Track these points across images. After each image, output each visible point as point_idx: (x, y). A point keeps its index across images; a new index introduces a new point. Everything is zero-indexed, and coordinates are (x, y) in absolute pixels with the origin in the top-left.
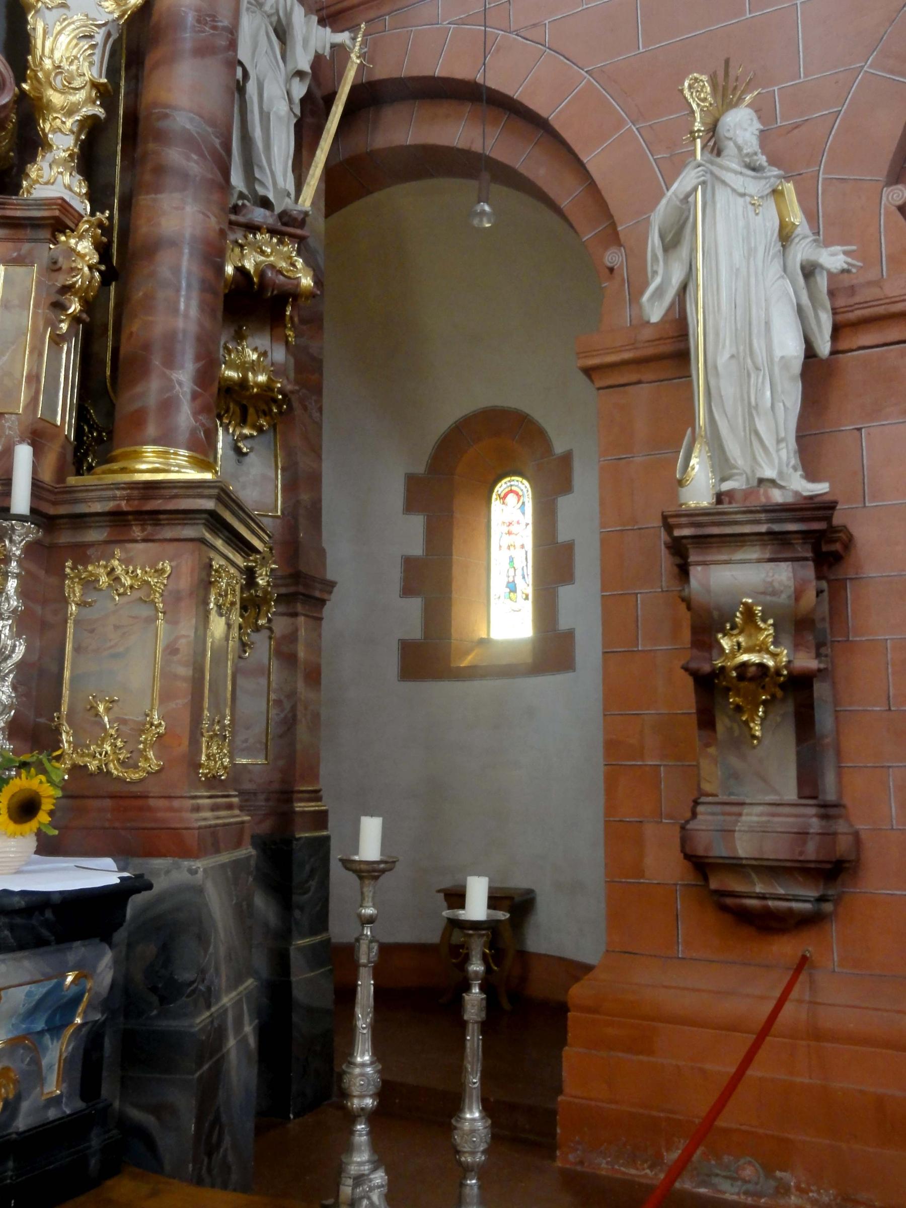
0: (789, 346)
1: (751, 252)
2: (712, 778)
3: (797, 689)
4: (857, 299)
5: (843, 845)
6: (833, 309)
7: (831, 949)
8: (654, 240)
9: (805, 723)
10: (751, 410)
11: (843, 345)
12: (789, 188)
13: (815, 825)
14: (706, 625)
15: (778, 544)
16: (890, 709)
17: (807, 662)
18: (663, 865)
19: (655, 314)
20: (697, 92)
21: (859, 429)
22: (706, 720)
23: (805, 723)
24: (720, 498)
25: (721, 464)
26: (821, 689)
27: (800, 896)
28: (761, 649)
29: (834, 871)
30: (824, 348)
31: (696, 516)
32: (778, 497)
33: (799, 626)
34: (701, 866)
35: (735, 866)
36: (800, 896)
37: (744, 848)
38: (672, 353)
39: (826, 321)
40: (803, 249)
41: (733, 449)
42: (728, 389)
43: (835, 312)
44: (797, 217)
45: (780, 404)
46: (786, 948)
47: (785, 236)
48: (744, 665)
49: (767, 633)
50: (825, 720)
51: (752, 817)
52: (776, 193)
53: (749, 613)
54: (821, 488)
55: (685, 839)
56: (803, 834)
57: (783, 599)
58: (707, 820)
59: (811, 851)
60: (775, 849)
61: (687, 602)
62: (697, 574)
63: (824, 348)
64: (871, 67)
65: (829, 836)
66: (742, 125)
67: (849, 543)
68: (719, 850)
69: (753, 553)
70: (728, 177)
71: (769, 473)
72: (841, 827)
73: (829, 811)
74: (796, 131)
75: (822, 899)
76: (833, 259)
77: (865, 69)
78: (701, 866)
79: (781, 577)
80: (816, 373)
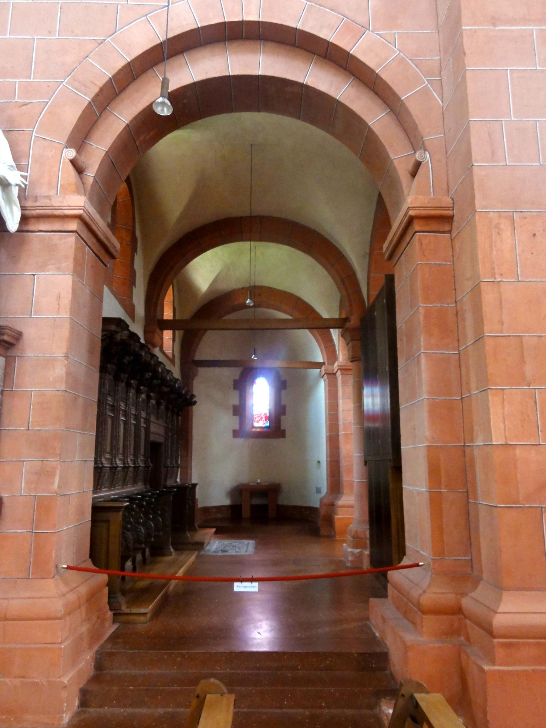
4: (38, 204)
6: (21, 207)
11: (31, 227)
16: (29, 429)
21: (34, 275)
43: (23, 208)
64: (66, 83)
67: (19, 336)
74: (24, 107)
77: (64, 83)
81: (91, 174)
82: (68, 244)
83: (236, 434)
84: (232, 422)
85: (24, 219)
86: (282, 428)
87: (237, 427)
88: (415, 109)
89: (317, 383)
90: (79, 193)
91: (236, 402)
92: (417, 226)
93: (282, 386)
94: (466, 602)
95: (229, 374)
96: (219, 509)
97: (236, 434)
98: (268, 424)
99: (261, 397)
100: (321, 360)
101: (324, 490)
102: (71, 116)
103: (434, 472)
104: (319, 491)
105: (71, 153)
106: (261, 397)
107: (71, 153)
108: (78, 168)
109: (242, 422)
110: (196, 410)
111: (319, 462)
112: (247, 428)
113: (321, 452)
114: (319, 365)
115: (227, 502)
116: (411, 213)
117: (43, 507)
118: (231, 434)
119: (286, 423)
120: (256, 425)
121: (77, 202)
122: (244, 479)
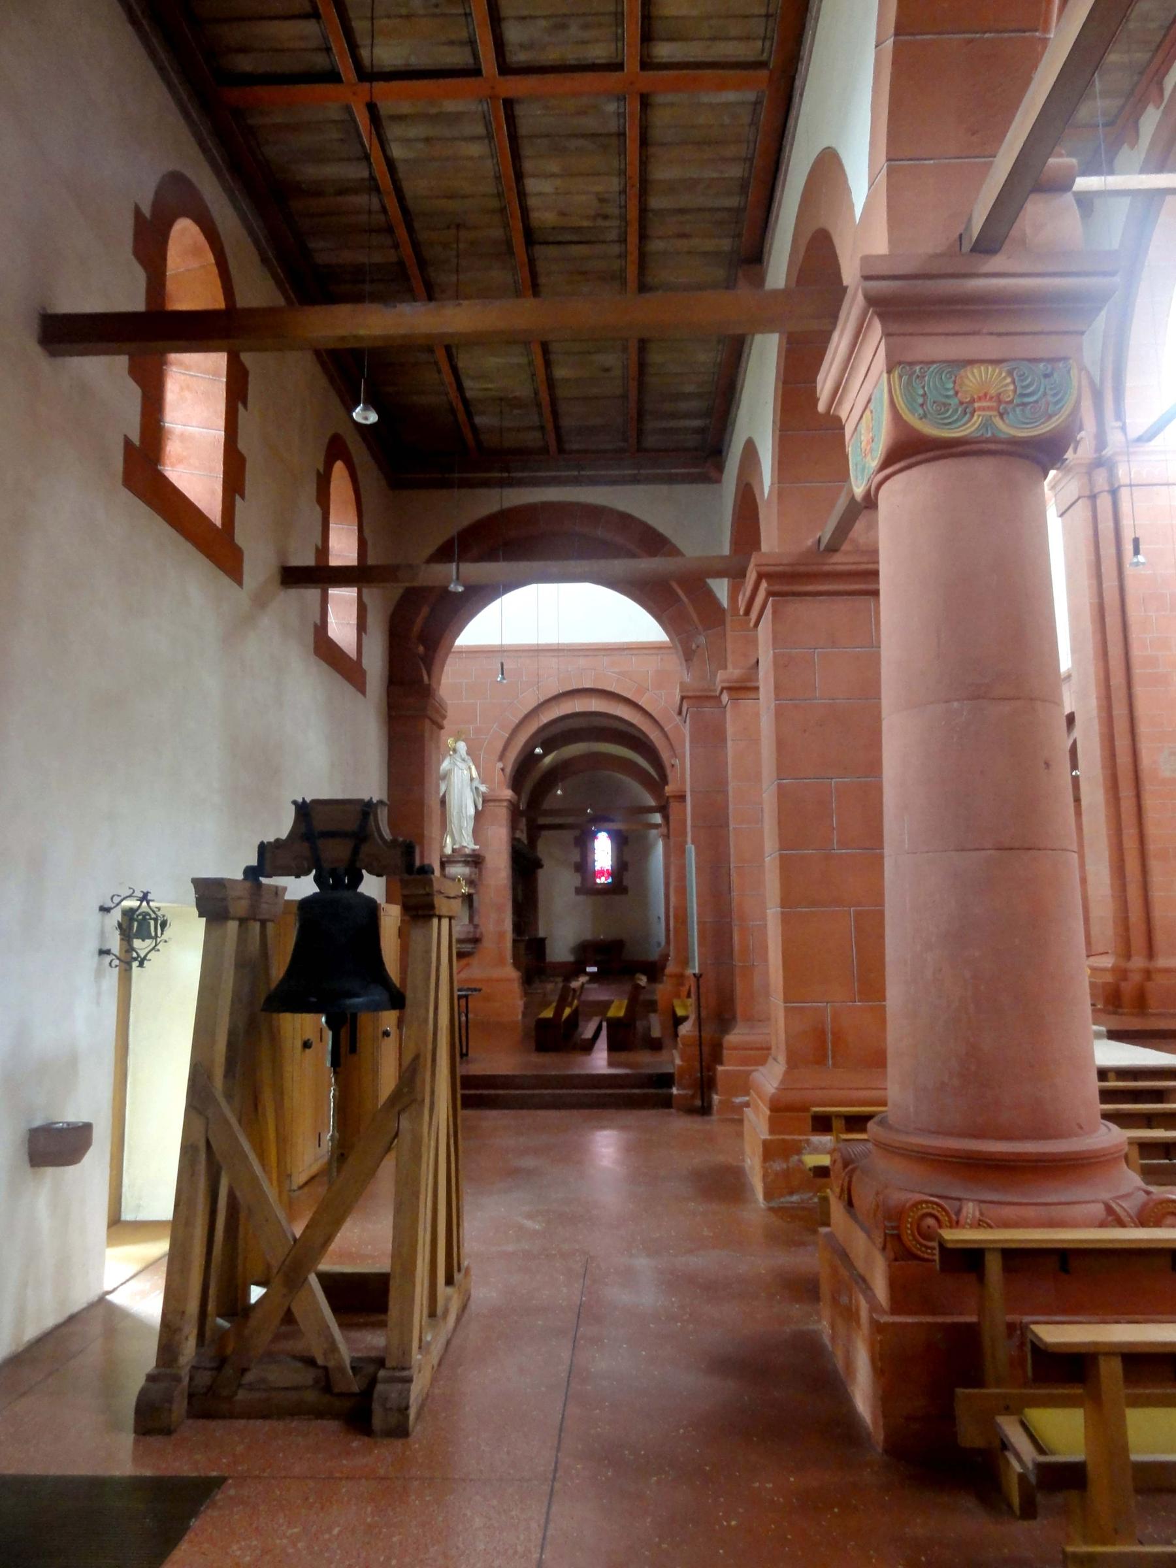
7: (474, 961)
9: (471, 906)
10: (461, 828)
12: (473, 768)
15: (466, 863)
17: (472, 891)
23: (471, 906)
24: (454, 850)
25: (454, 841)
26: (475, 897)
29: (476, 941)
30: (480, 808)
31: (448, 856)
32: (467, 851)
33: (471, 883)
42: (455, 820)
44: (475, 774)
45: (468, 825)
47: (472, 779)
50: (476, 904)
54: (477, 847)
56: (469, 932)
59: (471, 936)
62: (447, 870)
63: (480, 808)
66: (462, 746)
73: (476, 926)
76: (483, 788)
80: (478, 815)
81: (508, 770)
82: (502, 813)
83: (578, 891)
84: (575, 880)
85: (484, 801)
86: (625, 883)
88: (671, 735)
93: (621, 842)
95: (568, 836)
97: (578, 891)
98: (610, 880)
99: (603, 852)
101: (663, 944)
102: (499, 745)
104: (659, 944)
105: (500, 765)
106: (603, 852)
107: (500, 765)
108: (503, 770)
114: (657, 826)
115: (570, 958)
117: (501, 935)
120: (598, 881)
121: (508, 794)
122: (588, 936)
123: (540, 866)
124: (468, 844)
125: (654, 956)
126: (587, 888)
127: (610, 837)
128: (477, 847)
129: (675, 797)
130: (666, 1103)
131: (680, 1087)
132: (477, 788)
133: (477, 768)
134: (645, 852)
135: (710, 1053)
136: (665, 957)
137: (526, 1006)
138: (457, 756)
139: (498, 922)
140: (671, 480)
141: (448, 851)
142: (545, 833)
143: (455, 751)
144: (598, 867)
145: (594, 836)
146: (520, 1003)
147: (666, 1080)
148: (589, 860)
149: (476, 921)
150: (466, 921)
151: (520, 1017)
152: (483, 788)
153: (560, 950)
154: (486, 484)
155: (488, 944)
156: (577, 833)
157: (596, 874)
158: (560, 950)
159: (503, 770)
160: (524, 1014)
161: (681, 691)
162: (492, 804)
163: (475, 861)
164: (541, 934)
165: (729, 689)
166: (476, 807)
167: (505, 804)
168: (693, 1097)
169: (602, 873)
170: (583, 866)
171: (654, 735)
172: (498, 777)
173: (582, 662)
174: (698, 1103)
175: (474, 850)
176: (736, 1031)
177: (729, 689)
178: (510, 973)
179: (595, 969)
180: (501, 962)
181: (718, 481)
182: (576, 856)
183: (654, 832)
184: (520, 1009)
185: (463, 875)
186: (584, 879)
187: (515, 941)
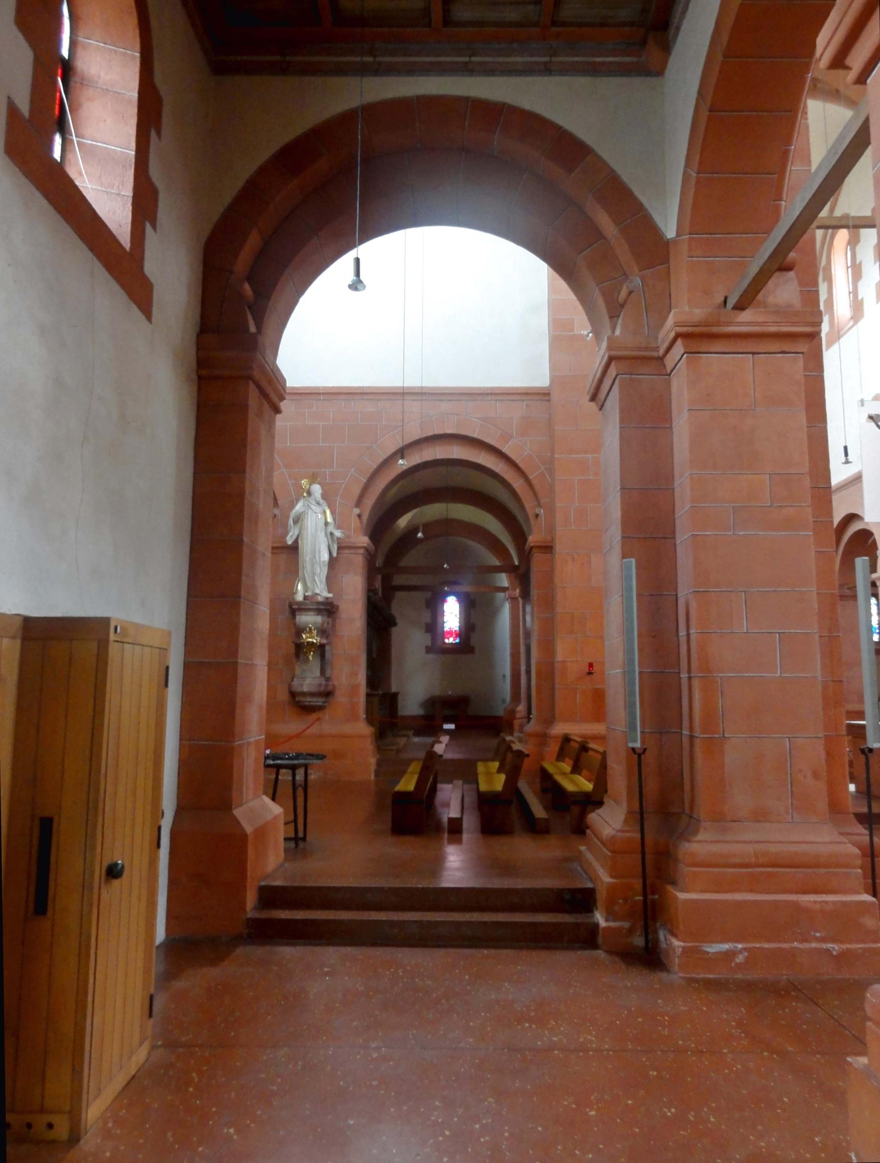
0: (325, 557)
1: (316, 531)
2: (298, 671)
3: (322, 647)
5: (330, 688)
7: (326, 716)
8: (291, 521)
10: (314, 574)
13: (324, 683)
14: (299, 631)
15: (319, 611)
17: (324, 641)
18: (283, 695)
19: (290, 542)
20: (304, 482)
22: (297, 655)
24: (305, 598)
26: (327, 648)
27: (318, 701)
28: (313, 638)
29: (328, 694)
30: (335, 554)
31: (299, 603)
32: (320, 599)
33: (322, 632)
34: (293, 695)
35: (303, 694)
36: (318, 701)
37: (305, 689)
38: (294, 549)
39: (336, 546)
40: (331, 528)
41: (309, 584)
42: (308, 566)
44: (330, 519)
45: (322, 572)
46: (314, 716)
47: (326, 524)
48: (308, 642)
49: (315, 632)
50: (328, 655)
51: (308, 681)
52: (324, 512)
53: (310, 629)
54: (331, 595)
55: (290, 686)
56: (320, 685)
57: (319, 625)
58: (296, 682)
60: (313, 689)
61: (295, 624)
62: (298, 617)
63: (335, 554)
65: (327, 685)
66: (317, 489)
67: (338, 606)
68: (299, 690)
69: (312, 613)
70: (312, 506)
71: (317, 591)
72: (331, 683)
73: (328, 679)
75: (324, 702)
76: (338, 534)
78: (293, 695)
79: (319, 619)
80: (333, 562)
81: (365, 517)
82: (359, 560)
83: (429, 650)
85: (339, 548)
86: (472, 643)
87: (429, 643)
89: (502, 606)
90: (365, 534)
91: (429, 620)
92: (534, 550)
93: (469, 606)
94: (548, 731)
96: (414, 718)
97: (429, 650)
98: (458, 641)
99: (452, 614)
100: (507, 585)
101: (508, 699)
102: (356, 491)
103: (538, 674)
104: (504, 701)
105: (357, 511)
106: (452, 614)
107: (357, 511)
108: (359, 516)
109: (434, 639)
110: (394, 630)
111: (504, 676)
112: (439, 643)
113: (505, 667)
114: (504, 589)
116: (531, 545)
117: (355, 688)
118: (424, 650)
119: (475, 641)
120: (446, 641)
121: (364, 540)
122: (437, 692)
123: (395, 624)
124: (322, 591)
125: (500, 712)
126: (436, 648)
127: (459, 601)
128: (331, 595)
129: (539, 547)
130: (589, 938)
131: (610, 915)
132: (332, 534)
133: (333, 513)
134: (492, 612)
135: (654, 869)
136: (513, 712)
137: (379, 764)
138: (311, 500)
139: (351, 673)
140: (594, 70)
141: (299, 597)
142: (399, 595)
143: (309, 493)
144: (447, 628)
145: (444, 601)
146: (373, 761)
147: (582, 900)
148: (439, 620)
149: (328, 673)
150: (318, 674)
151: (373, 777)
152: (338, 534)
153: (412, 703)
154: (341, 71)
155: (341, 698)
156: (428, 595)
157: (445, 635)
158: (412, 703)
159: (359, 516)
160: (377, 774)
161: (609, 348)
162: (346, 551)
163: (329, 609)
164: (394, 690)
165: (685, 336)
166: (330, 553)
167: (362, 551)
168: (631, 931)
169: (450, 633)
170: (433, 626)
171: (517, 484)
172: (354, 523)
173: (445, 406)
174: (639, 941)
175: (327, 598)
176: (700, 837)
177: (685, 336)
178: (363, 729)
179: (452, 726)
180: (354, 717)
181: (659, 72)
182: (426, 617)
183: (501, 595)
184: (373, 768)
185: (314, 624)
186: (434, 639)
187: (368, 695)
